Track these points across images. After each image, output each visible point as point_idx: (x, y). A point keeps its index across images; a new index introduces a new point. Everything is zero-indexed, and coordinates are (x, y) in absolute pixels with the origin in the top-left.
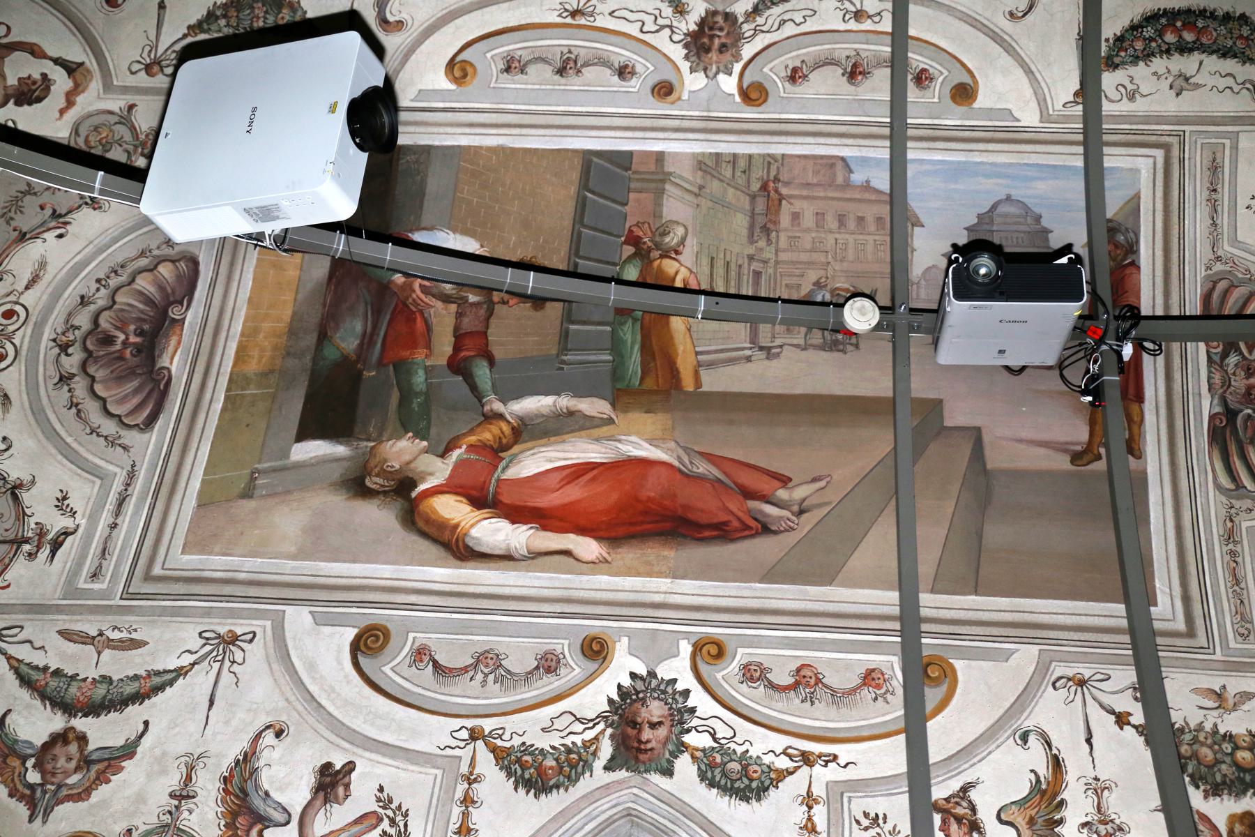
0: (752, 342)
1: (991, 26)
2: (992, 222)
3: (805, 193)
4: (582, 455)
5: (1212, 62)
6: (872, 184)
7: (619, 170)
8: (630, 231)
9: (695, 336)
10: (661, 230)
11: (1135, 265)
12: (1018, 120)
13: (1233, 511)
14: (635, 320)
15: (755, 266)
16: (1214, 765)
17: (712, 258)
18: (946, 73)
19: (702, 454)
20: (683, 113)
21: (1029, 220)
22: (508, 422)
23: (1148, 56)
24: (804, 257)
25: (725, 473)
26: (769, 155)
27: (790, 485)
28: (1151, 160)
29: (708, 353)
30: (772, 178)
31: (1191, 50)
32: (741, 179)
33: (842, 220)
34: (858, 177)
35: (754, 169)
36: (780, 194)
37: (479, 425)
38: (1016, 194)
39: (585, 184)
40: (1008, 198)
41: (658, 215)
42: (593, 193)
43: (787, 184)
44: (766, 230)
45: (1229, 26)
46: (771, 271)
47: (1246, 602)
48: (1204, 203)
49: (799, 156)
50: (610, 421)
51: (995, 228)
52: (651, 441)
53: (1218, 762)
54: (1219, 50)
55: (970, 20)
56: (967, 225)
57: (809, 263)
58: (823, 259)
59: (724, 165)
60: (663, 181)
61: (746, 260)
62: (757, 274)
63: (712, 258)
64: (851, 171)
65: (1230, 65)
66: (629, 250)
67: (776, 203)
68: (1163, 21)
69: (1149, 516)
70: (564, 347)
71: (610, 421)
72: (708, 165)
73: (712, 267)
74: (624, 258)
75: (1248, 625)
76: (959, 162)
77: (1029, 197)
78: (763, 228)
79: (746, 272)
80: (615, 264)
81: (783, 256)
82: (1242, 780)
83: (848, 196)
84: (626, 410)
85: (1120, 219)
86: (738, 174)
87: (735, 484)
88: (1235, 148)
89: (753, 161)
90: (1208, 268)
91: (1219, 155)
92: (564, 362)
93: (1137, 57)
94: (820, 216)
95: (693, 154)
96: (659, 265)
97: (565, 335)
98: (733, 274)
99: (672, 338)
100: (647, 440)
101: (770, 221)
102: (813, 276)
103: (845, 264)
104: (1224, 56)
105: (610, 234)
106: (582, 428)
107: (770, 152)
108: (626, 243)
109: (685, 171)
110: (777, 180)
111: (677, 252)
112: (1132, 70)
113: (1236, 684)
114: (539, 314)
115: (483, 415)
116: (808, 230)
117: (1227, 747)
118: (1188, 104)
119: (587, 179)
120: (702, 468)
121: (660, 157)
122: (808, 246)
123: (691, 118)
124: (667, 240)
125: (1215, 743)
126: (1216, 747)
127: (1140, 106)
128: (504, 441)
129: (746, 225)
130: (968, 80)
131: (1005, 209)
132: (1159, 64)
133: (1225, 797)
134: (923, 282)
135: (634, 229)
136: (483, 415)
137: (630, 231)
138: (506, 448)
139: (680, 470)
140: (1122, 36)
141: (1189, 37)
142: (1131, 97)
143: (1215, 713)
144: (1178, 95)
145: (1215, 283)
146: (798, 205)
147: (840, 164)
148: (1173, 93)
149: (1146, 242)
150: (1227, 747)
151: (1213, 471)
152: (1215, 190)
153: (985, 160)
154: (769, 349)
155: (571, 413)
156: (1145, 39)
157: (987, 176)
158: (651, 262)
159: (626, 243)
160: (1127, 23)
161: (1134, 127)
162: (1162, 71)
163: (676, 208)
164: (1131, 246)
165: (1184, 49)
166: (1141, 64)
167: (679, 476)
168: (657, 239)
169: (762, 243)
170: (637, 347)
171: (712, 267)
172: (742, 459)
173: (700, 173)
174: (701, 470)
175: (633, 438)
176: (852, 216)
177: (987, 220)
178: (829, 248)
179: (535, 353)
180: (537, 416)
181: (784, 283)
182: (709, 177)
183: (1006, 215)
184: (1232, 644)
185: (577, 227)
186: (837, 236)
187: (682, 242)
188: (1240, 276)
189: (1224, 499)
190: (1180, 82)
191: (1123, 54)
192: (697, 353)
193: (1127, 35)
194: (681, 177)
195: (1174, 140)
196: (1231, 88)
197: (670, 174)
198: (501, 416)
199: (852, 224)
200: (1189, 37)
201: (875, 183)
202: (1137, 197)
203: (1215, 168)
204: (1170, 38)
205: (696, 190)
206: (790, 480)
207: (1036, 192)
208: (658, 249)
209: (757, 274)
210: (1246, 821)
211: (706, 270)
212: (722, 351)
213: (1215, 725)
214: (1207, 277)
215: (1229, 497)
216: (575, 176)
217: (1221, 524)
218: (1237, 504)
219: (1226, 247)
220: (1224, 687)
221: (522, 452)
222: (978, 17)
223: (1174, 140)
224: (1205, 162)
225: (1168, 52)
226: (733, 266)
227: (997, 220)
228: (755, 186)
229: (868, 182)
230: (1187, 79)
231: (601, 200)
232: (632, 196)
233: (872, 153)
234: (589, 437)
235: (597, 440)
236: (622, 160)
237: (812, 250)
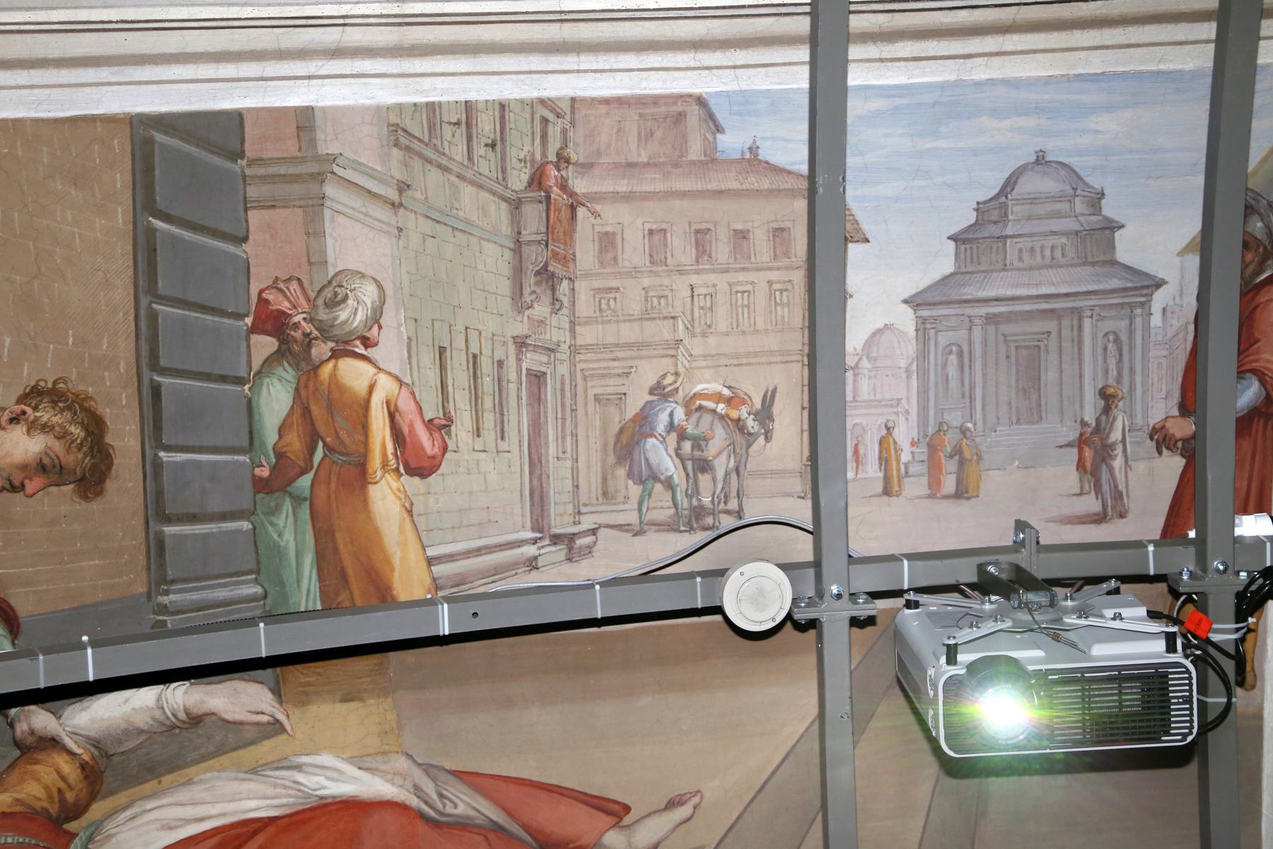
0: (538, 526)
3: (623, 186)
4: (230, 807)
6: (764, 154)
7: (217, 160)
8: (262, 302)
9: (422, 523)
10: (328, 293)
14: (297, 500)
15: (533, 360)
17: (442, 350)
19: (458, 774)
20: (345, 9)
21: (1080, 206)
22: (71, 753)
24: (629, 333)
25: (510, 814)
26: (542, 101)
27: (627, 820)
29: (451, 558)
30: (552, 157)
32: (486, 164)
33: (701, 239)
34: (732, 142)
35: (513, 137)
36: (572, 194)
37: (12, 766)
38: (1057, 148)
39: (146, 199)
40: (1040, 159)
41: (316, 260)
42: (167, 218)
43: (586, 167)
44: (547, 277)
46: (563, 369)
49: (606, 101)
50: (276, 728)
51: (1009, 231)
52: (360, 761)
56: (954, 230)
57: (639, 346)
58: (667, 335)
59: (448, 130)
60: (319, 178)
61: (512, 349)
62: (537, 378)
63: (442, 350)
64: (719, 129)
66: (265, 345)
67: (565, 214)
69: (1260, 804)
70: (160, 580)
71: (276, 728)
72: (416, 135)
73: (443, 368)
74: (256, 364)
76: (943, 86)
78: (542, 268)
79: (513, 375)
80: (240, 381)
81: (587, 335)
83: (713, 186)
84: (303, 700)
86: (479, 150)
87: (526, 828)
89: (510, 117)
92: (163, 609)
94: (657, 235)
95: (378, 110)
96: (334, 375)
97: (157, 548)
98: (487, 383)
99: (377, 532)
100: (351, 760)
101: (555, 255)
102: (648, 373)
103: (712, 340)
105: (222, 313)
106: (221, 750)
107: (545, 94)
108: (254, 329)
109: (364, 151)
110: (563, 160)
111: (367, 342)
114: (95, 506)
115: (17, 744)
116: (635, 273)
119: (149, 188)
120: (465, 804)
121: (304, 120)
122: (636, 308)
123: (364, 21)
124: (343, 316)
128: (70, 797)
129: (506, 270)
131: (1033, 184)
134: (865, 364)
135: (268, 296)
136: (17, 744)
137: (262, 302)
138: (76, 811)
139: (422, 815)
146: (612, 215)
147: (694, 111)
153: (996, 75)
154: (572, 537)
155: (195, 720)
158: (316, 368)
159: (254, 329)
163: (358, 245)
167: (421, 827)
168: (323, 315)
169: (541, 310)
170: (309, 559)
171: (443, 368)
172: (535, 777)
173: (395, 152)
174: (461, 809)
175: (326, 759)
176: (723, 233)
177: (995, 215)
178: (677, 311)
179: (100, 596)
180: (126, 732)
181: (591, 393)
182: (417, 163)
183: (1033, 200)
185: (144, 301)
186: (694, 279)
187: (376, 319)
192: (430, 562)
194: (357, 166)
197: (333, 159)
198: (52, 743)
199: (722, 251)
201: (770, 153)
205: (392, 194)
206: (627, 809)
207: (1093, 139)
208: (326, 339)
209: (537, 378)
211: (432, 376)
212: (478, 552)
216: (121, 179)
221: (110, 815)
226: (486, 365)
227: (1016, 211)
228: (519, 179)
229: (753, 149)
231: (187, 235)
232: (255, 217)
233: (761, 81)
234: (238, 767)
235: (254, 771)
236: (221, 132)
237: (647, 316)
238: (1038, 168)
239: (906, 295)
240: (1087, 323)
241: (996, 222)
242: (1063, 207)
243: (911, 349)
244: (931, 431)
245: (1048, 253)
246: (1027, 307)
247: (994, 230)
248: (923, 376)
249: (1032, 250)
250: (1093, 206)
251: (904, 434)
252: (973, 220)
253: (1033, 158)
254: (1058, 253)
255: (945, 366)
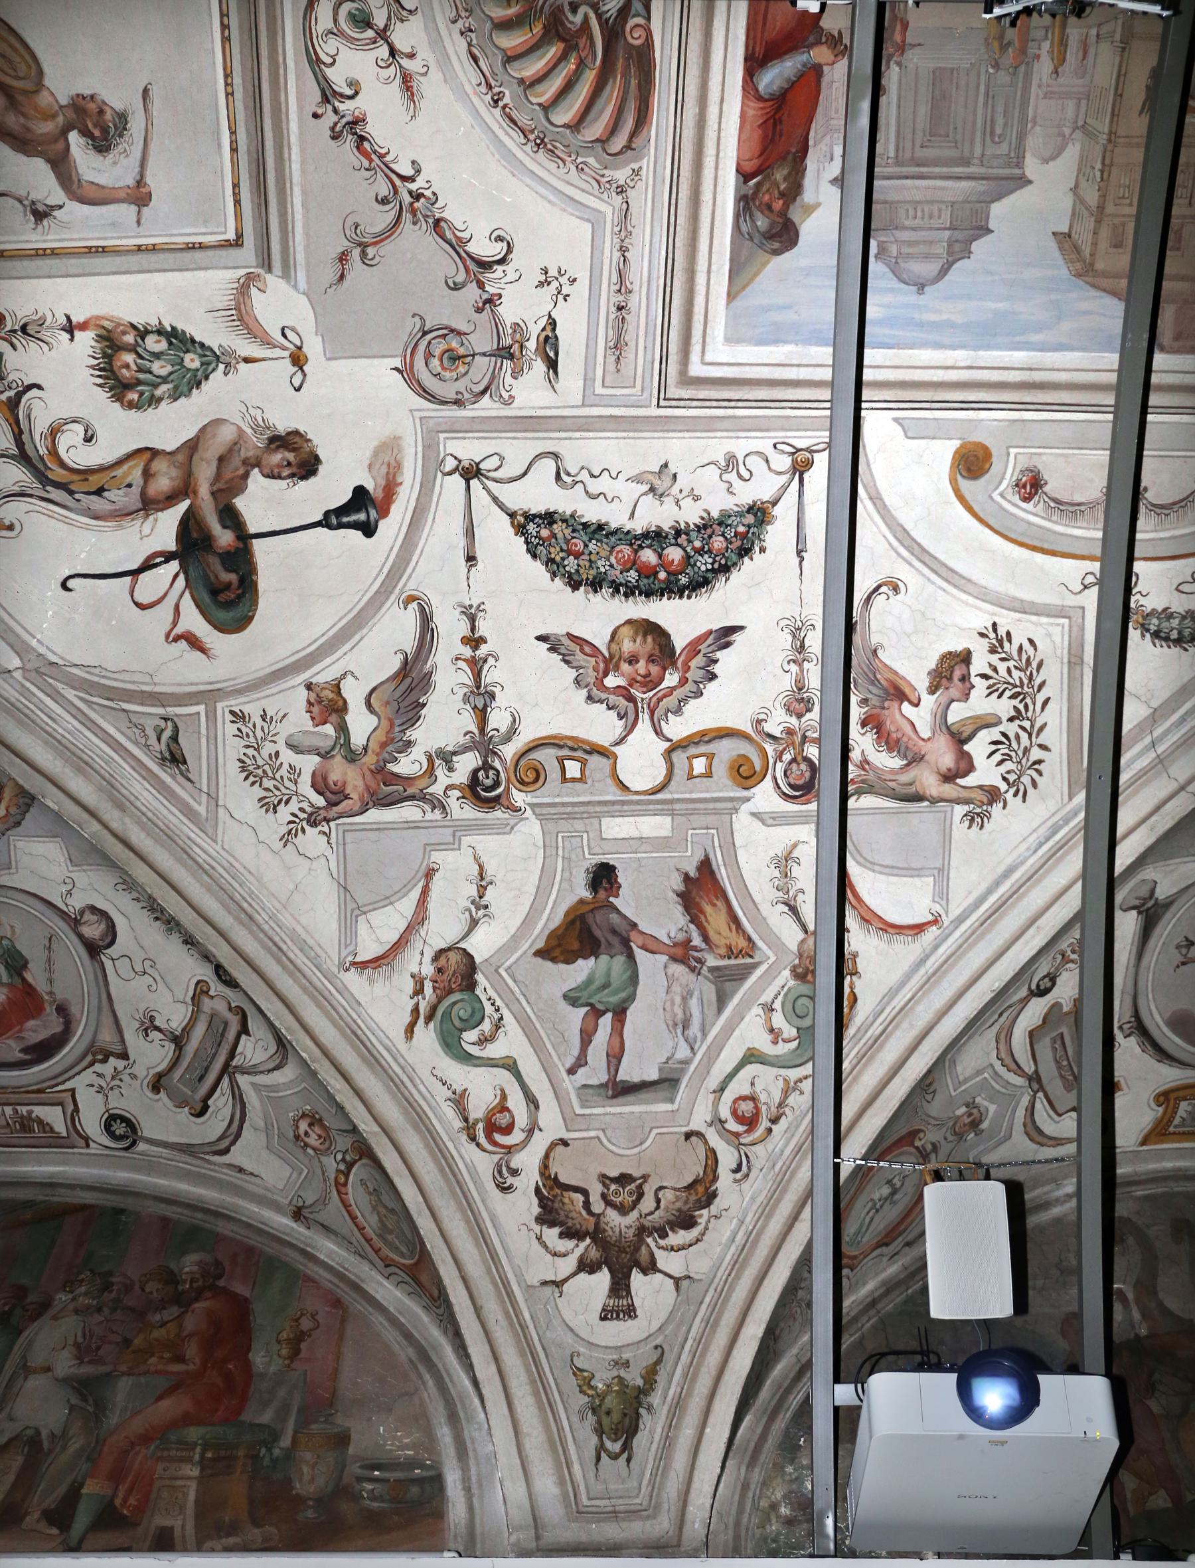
1: (926, 571)
2: (951, 244)
5: (616, 517)
11: (744, 175)
12: (896, 420)
18: (996, 496)
21: (894, 249)
23: (705, 527)
28: (709, 357)
31: (646, 535)
40: (921, 287)
45: (593, 572)
48: (636, 288)
51: (947, 233)
54: (607, 536)
55: (956, 580)
65: (592, 512)
68: (684, 580)
77: (892, 290)
85: (762, 256)
88: (588, 380)
90: (636, 172)
91: (611, 367)
93: (720, 524)
104: (600, 527)
112: (729, 503)
118: (650, 451)
127: (719, 446)
130: (965, 485)
131: (928, 269)
132: (691, 515)
140: (741, 556)
141: (648, 556)
142: (731, 461)
144: (666, 465)
145: (628, 147)
148: (672, 468)
149: (724, 216)
152: (620, 308)
156: (710, 551)
157: (951, 325)
160: (735, 575)
161: (730, 412)
162: (687, 503)
164: (747, 208)
165: (656, 537)
166: (715, 514)
177: (957, 247)
183: (927, 257)
188: (591, 161)
190: (662, 484)
191: (741, 529)
193: (734, 558)
195: (673, 392)
196: (592, 476)
200: (648, 556)
202: (731, 297)
203: (618, 346)
204: (674, 554)
214: (639, 158)
219: (608, 210)
222: (945, 585)
223: (673, 392)
224: (632, 356)
225: (678, 533)
227: (941, 249)
230: (652, 489)
238: (921, 281)
239: (1030, 187)
240: (892, 154)
241: (957, 241)
242: (906, 250)
243: (1031, 142)
244: (1022, 68)
245: (919, 214)
246: (937, 170)
247: (958, 235)
248: (1023, 120)
249: (931, 217)
250: (884, 249)
251: (1044, 67)
252: (974, 245)
253: (926, 289)
254: (911, 212)
255: (1006, 125)
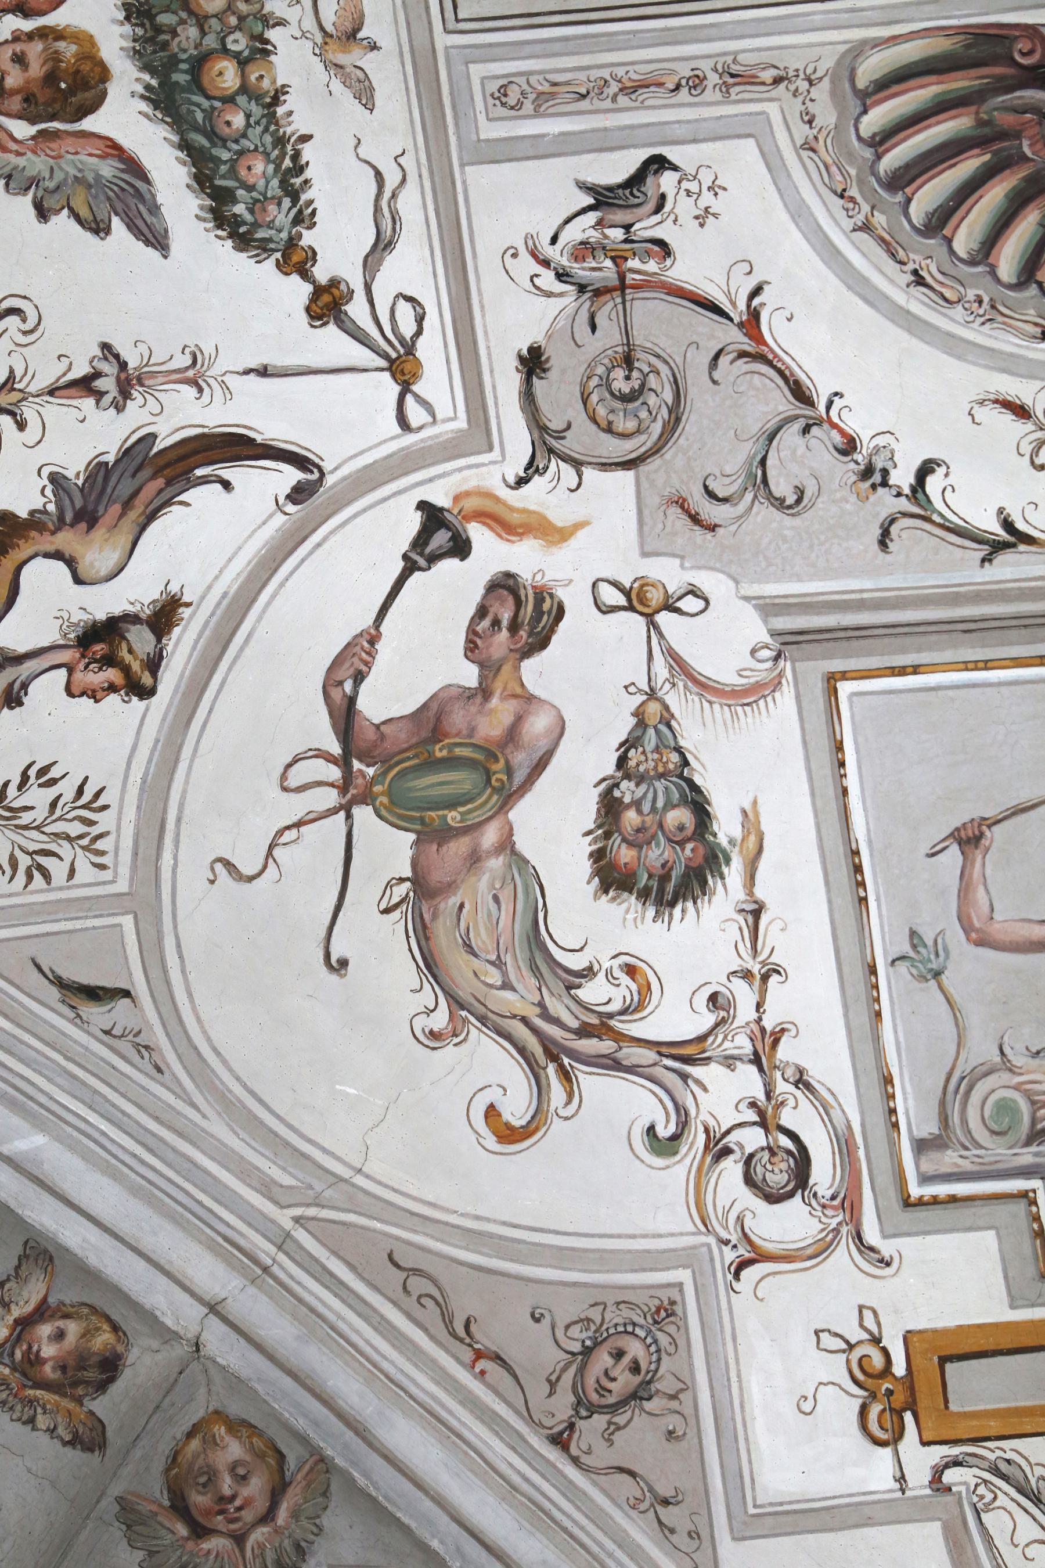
13: (803, 85)
16: (191, 13)
47: (585, 104)
53: (201, 21)
75: (528, 107)
82: (173, 62)
113: (386, 71)
117: (238, 43)
125: (241, 19)
126: (233, 21)
133: (127, 28)
143: (309, 24)
150: (238, 43)
151: (894, 40)
184: (477, 71)
189: (827, 63)
210: (86, 67)
213: (282, 23)
215: (834, 76)
217: (765, 57)
218: (822, 92)
220: (374, 47)
